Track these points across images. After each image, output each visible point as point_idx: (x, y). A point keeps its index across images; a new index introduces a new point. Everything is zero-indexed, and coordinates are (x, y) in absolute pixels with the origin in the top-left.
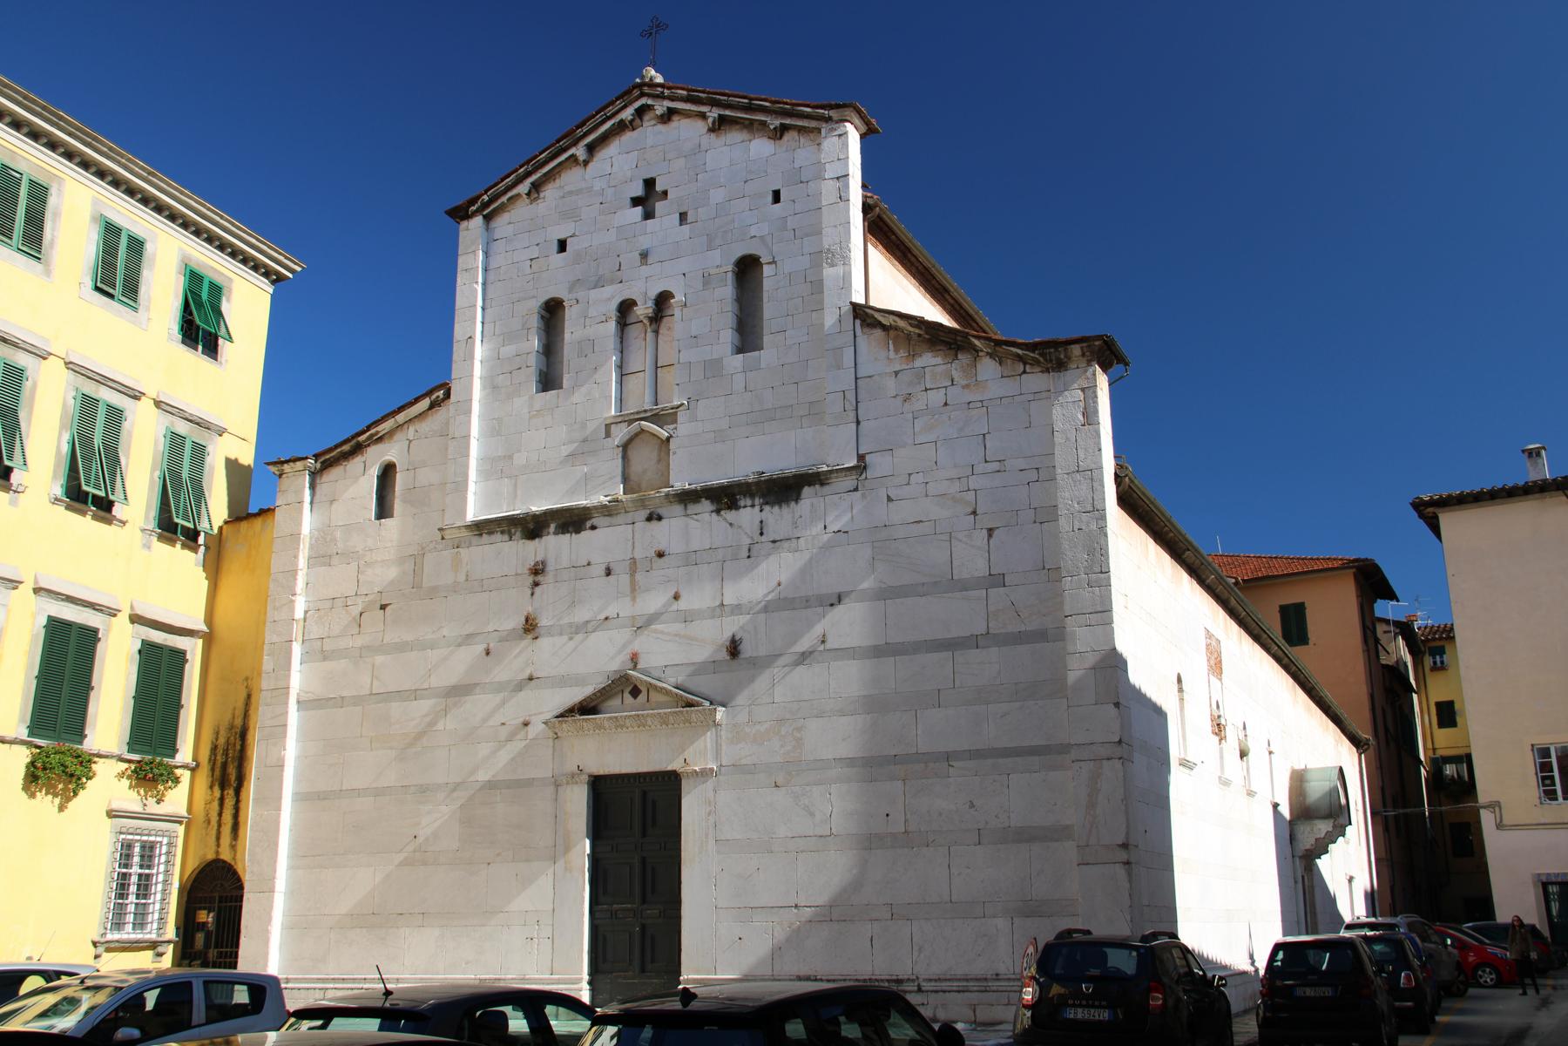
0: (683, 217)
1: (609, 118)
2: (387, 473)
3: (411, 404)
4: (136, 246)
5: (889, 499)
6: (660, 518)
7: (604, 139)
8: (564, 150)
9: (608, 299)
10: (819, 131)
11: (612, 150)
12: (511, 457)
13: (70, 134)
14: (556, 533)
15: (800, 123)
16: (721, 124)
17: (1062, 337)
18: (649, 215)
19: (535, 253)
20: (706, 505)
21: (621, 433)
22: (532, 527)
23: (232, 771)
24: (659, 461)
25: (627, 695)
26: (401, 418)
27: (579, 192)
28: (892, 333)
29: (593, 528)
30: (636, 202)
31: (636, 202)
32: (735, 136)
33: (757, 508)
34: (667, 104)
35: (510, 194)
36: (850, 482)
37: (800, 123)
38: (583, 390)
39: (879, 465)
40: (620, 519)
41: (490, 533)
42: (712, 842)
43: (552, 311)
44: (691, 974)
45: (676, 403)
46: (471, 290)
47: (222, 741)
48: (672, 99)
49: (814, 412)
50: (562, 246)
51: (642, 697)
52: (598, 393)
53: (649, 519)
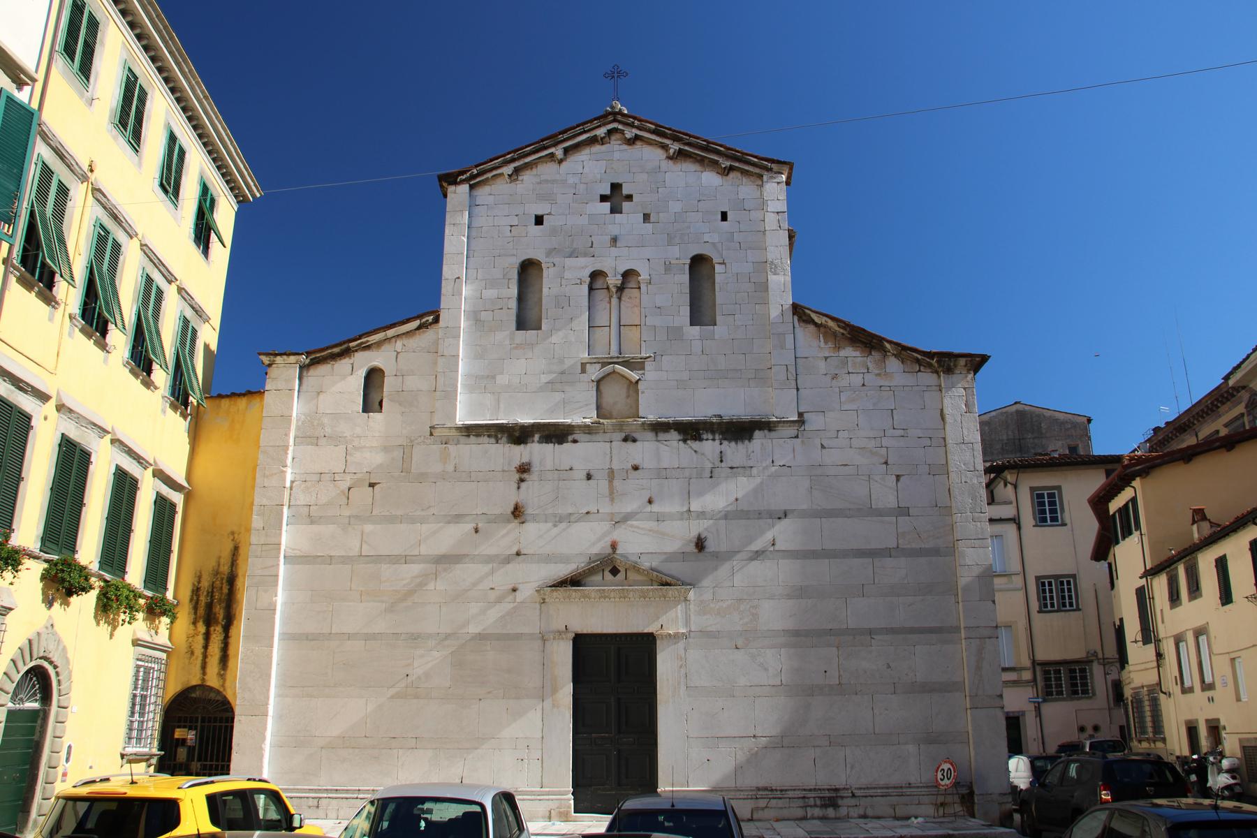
0: (646, 217)
1: (585, 132)
3: (403, 323)
6: (634, 441)
7: (577, 147)
8: (545, 148)
9: (582, 268)
10: (761, 176)
11: (584, 155)
12: (494, 377)
14: (540, 442)
15: (746, 168)
16: (681, 155)
17: (956, 351)
18: (615, 210)
20: (674, 435)
21: (595, 372)
22: (519, 435)
23: (219, 611)
24: (628, 397)
26: (391, 333)
27: (553, 182)
28: (822, 329)
29: (575, 441)
30: (604, 198)
31: (604, 198)
32: (689, 167)
33: (717, 442)
34: (635, 131)
35: (495, 173)
36: (792, 431)
37: (746, 168)
38: (561, 334)
39: (814, 422)
40: (599, 437)
41: (477, 435)
42: (683, 688)
43: (528, 270)
44: (665, 786)
45: (644, 355)
46: (455, 240)
47: (205, 584)
49: (760, 377)
50: (539, 220)
51: (621, 576)
52: (569, 337)
53: (625, 440)
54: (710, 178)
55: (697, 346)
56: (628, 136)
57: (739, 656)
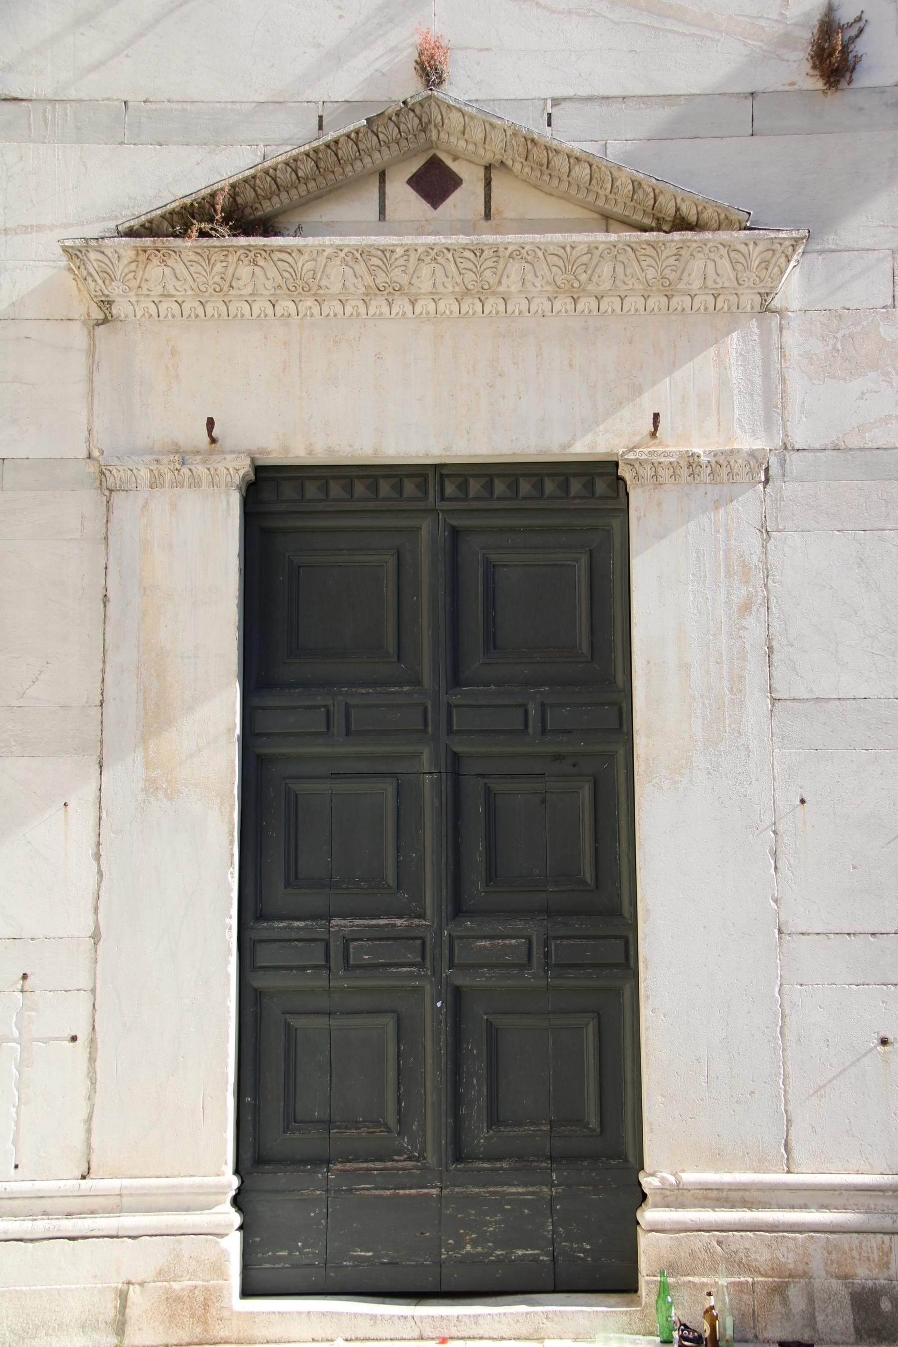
42: (756, 703)
51: (464, 201)
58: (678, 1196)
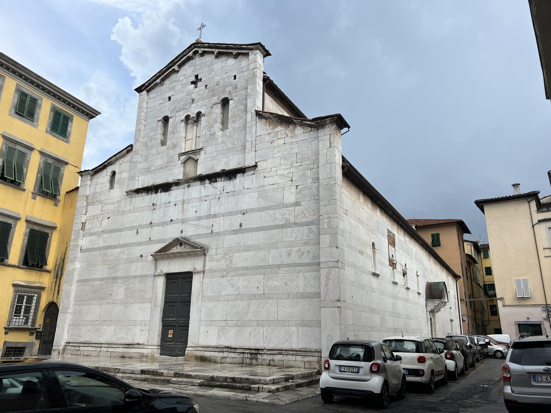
2: (114, 173)
4: (34, 101)
5: (265, 177)
8: (171, 67)
10: (248, 54)
13: (6, 61)
18: (196, 87)
19: (161, 101)
21: (183, 158)
25: (178, 246)
28: (268, 120)
30: (193, 83)
31: (193, 83)
32: (223, 59)
36: (252, 172)
40: (181, 187)
42: (201, 296)
47: (58, 262)
48: (204, 48)
50: (170, 98)
54: (231, 61)
55: (220, 140)
56: (200, 52)
57: (223, 280)
58: (189, 347)
